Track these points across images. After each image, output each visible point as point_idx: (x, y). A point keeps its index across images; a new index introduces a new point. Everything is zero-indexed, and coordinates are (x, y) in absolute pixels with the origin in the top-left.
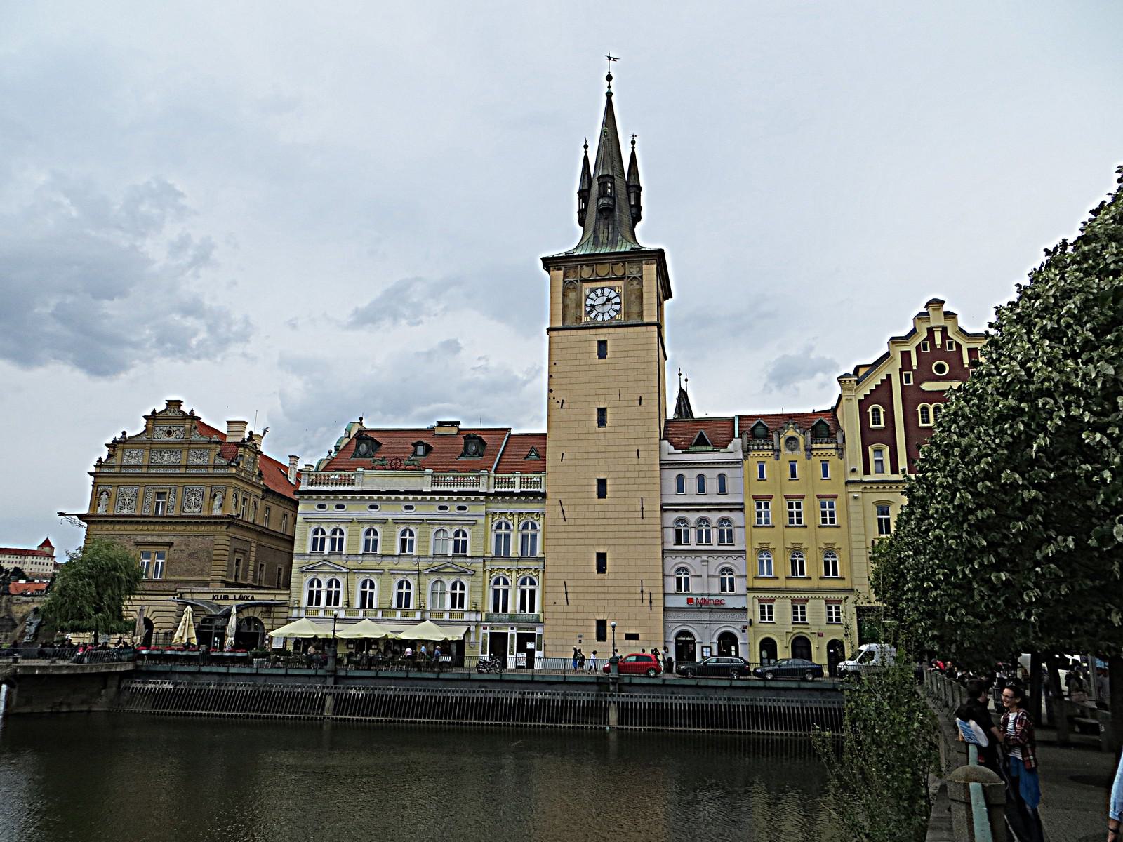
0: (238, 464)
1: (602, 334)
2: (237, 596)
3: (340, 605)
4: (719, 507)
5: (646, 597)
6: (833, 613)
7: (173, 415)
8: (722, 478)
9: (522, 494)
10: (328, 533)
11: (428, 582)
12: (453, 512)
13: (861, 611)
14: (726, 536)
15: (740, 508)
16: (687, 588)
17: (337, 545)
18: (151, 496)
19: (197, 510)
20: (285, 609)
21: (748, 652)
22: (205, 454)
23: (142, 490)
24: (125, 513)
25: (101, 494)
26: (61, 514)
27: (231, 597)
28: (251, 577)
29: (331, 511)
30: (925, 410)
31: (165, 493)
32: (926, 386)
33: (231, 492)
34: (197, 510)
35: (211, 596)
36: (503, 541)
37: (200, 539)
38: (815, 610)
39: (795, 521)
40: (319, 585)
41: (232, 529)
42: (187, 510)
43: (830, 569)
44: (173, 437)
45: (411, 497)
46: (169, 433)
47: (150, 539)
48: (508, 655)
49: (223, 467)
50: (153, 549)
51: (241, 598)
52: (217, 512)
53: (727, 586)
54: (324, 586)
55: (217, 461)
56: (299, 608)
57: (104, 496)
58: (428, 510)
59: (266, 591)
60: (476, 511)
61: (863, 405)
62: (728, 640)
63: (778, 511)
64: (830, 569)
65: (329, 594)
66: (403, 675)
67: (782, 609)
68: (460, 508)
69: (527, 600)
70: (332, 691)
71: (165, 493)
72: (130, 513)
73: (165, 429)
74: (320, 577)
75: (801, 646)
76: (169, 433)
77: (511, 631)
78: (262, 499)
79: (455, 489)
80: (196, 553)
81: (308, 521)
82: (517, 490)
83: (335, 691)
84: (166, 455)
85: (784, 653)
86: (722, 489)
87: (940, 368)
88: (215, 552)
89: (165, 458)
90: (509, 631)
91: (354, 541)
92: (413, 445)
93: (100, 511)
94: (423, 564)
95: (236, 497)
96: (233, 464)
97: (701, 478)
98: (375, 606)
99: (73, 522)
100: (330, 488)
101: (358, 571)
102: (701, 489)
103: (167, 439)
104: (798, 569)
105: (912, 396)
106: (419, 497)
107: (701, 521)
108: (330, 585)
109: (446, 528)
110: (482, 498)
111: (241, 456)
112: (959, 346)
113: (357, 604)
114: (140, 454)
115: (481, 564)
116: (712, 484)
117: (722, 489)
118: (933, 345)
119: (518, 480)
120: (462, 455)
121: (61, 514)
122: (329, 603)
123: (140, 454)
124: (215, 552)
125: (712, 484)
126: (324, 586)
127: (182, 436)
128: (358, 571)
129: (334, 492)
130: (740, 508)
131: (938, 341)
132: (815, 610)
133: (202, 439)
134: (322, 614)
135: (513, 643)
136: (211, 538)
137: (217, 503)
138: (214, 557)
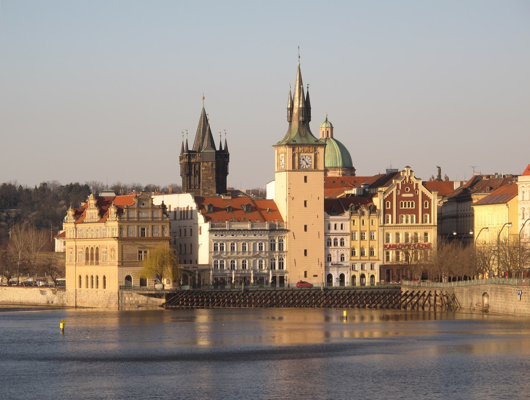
1: (306, 174)
4: (340, 234)
5: (320, 263)
6: (372, 268)
8: (342, 225)
13: (381, 267)
14: (342, 244)
15: (346, 234)
16: (331, 260)
17: (222, 248)
21: (347, 280)
30: (402, 203)
32: (404, 195)
36: (272, 247)
38: (367, 266)
39: (362, 238)
40: (217, 262)
43: (372, 253)
53: (342, 259)
54: (219, 262)
61: (384, 201)
62: (342, 276)
63: (357, 236)
64: (372, 253)
67: (358, 267)
69: (281, 265)
75: (363, 276)
77: (278, 275)
85: (358, 280)
86: (342, 228)
87: (407, 189)
91: (227, 247)
97: (335, 225)
100: (219, 229)
102: (335, 228)
104: (362, 254)
105: (399, 198)
107: (336, 239)
112: (413, 182)
116: (339, 227)
117: (342, 228)
118: (406, 182)
125: (339, 227)
126: (219, 262)
129: (220, 230)
130: (346, 234)
131: (407, 180)
132: (367, 266)
134: (219, 272)
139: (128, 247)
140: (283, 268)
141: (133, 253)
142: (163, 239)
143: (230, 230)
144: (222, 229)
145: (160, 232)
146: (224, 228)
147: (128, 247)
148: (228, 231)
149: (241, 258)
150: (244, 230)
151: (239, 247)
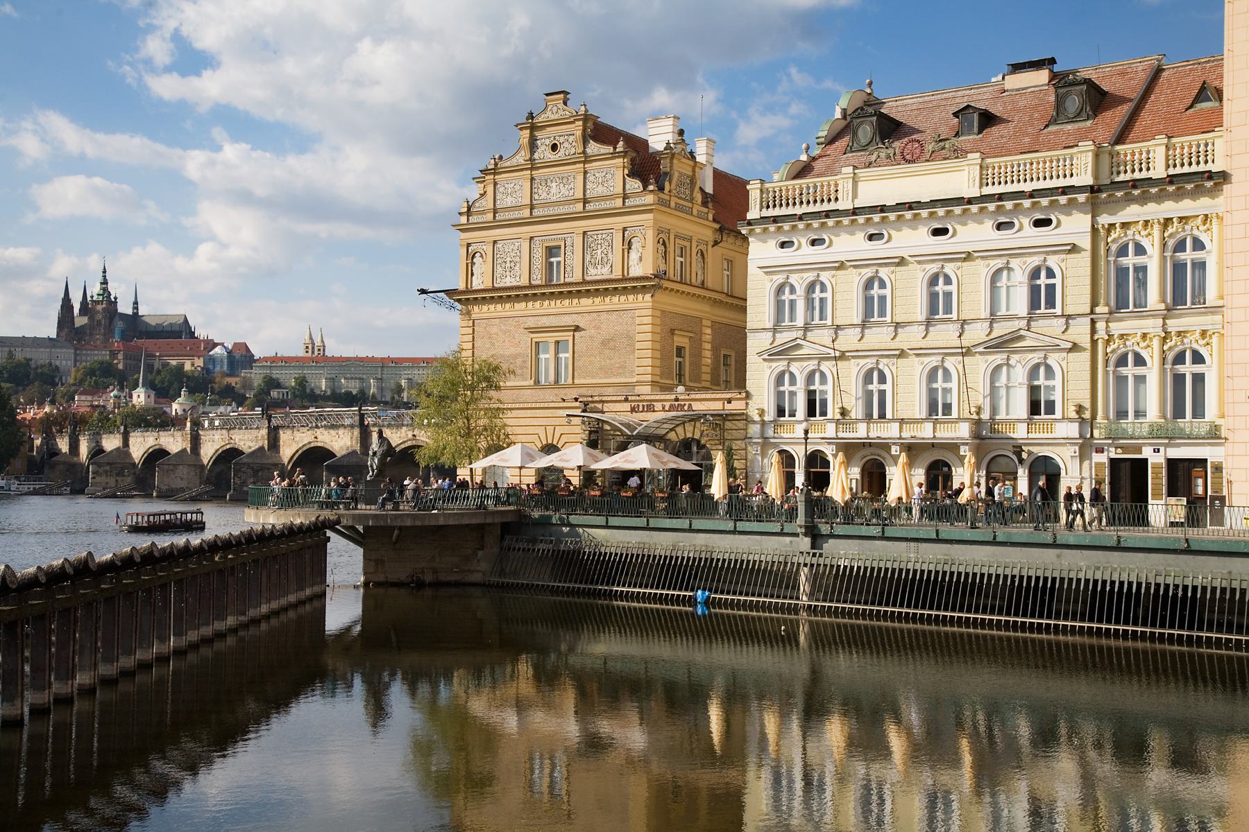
0: (661, 189)
2: (667, 405)
3: (830, 416)
7: (556, 117)
9: (1172, 179)
10: (801, 291)
11: (980, 366)
12: (1027, 234)
18: (539, 254)
19: (606, 270)
20: (741, 424)
22: (609, 176)
23: (526, 245)
24: (508, 284)
25: (473, 257)
26: (423, 292)
27: (658, 406)
28: (708, 377)
29: (805, 253)
31: (559, 247)
33: (650, 234)
34: (606, 270)
35: (627, 406)
37: (615, 315)
41: (660, 296)
42: (592, 271)
44: (561, 154)
45: (941, 212)
46: (554, 147)
47: (545, 321)
48: (1150, 501)
49: (637, 194)
50: (551, 338)
51: (672, 408)
52: (636, 270)
55: (628, 186)
56: (763, 423)
57: (477, 260)
58: (976, 233)
59: (708, 396)
60: (1075, 227)
65: (811, 395)
66: (686, 526)
68: (1039, 223)
69: (1185, 393)
70: (808, 560)
71: (559, 247)
72: (515, 284)
73: (547, 141)
74: (795, 368)
76: (554, 147)
77: (1155, 458)
78: (716, 243)
79: (1028, 187)
80: (612, 339)
81: (769, 270)
82: (1158, 172)
83: (814, 561)
84: (554, 184)
88: (639, 337)
89: (554, 190)
90: (1147, 453)
92: (956, 114)
93: (477, 284)
94: (976, 333)
95: (664, 244)
96: (651, 188)
98: (889, 415)
99: (441, 303)
100: (798, 210)
101: (858, 355)
103: (551, 156)
106: (957, 210)
108: (810, 378)
109: (1014, 263)
110: (1082, 198)
111: (666, 174)
113: (857, 412)
114: (517, 187)
115: (1087, 329)
119: (1159, 155)
120: (1053, 121)
121: (423, 292)
122: (811, 412)
123: (517, 187)
124: (639, 337)
127: (573, 151)
128: (858, 355)
133: (603, 151)
135: (1156, 480)
136: (630, 313)
137: (634, 256)
138: (638, 345)
139: (494, 330)
140: (1199, 411)
141: (512, 351)
142: (625, 286)
143: (855, 212)
144: (826, 207)
145: (616, 257)
146: (832, 206)
147: (494, 330)
148: (845, 213)
149: (920, 352)
150: (934, 203)
151: (908, 294)
